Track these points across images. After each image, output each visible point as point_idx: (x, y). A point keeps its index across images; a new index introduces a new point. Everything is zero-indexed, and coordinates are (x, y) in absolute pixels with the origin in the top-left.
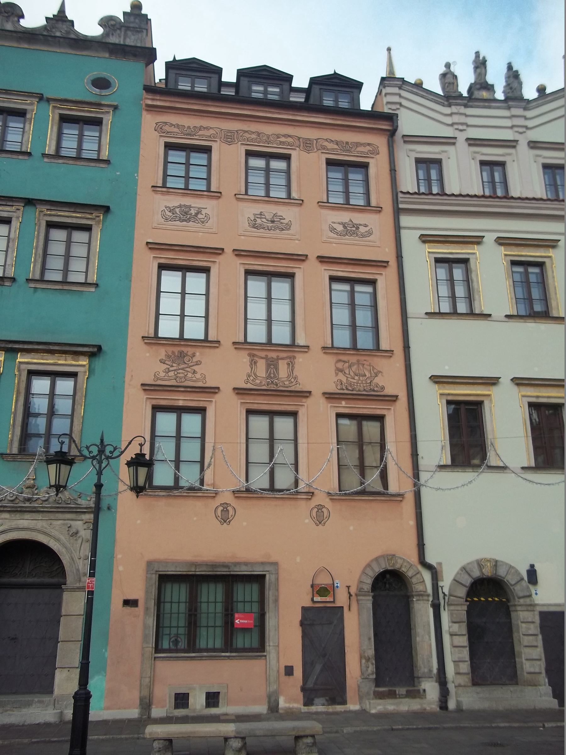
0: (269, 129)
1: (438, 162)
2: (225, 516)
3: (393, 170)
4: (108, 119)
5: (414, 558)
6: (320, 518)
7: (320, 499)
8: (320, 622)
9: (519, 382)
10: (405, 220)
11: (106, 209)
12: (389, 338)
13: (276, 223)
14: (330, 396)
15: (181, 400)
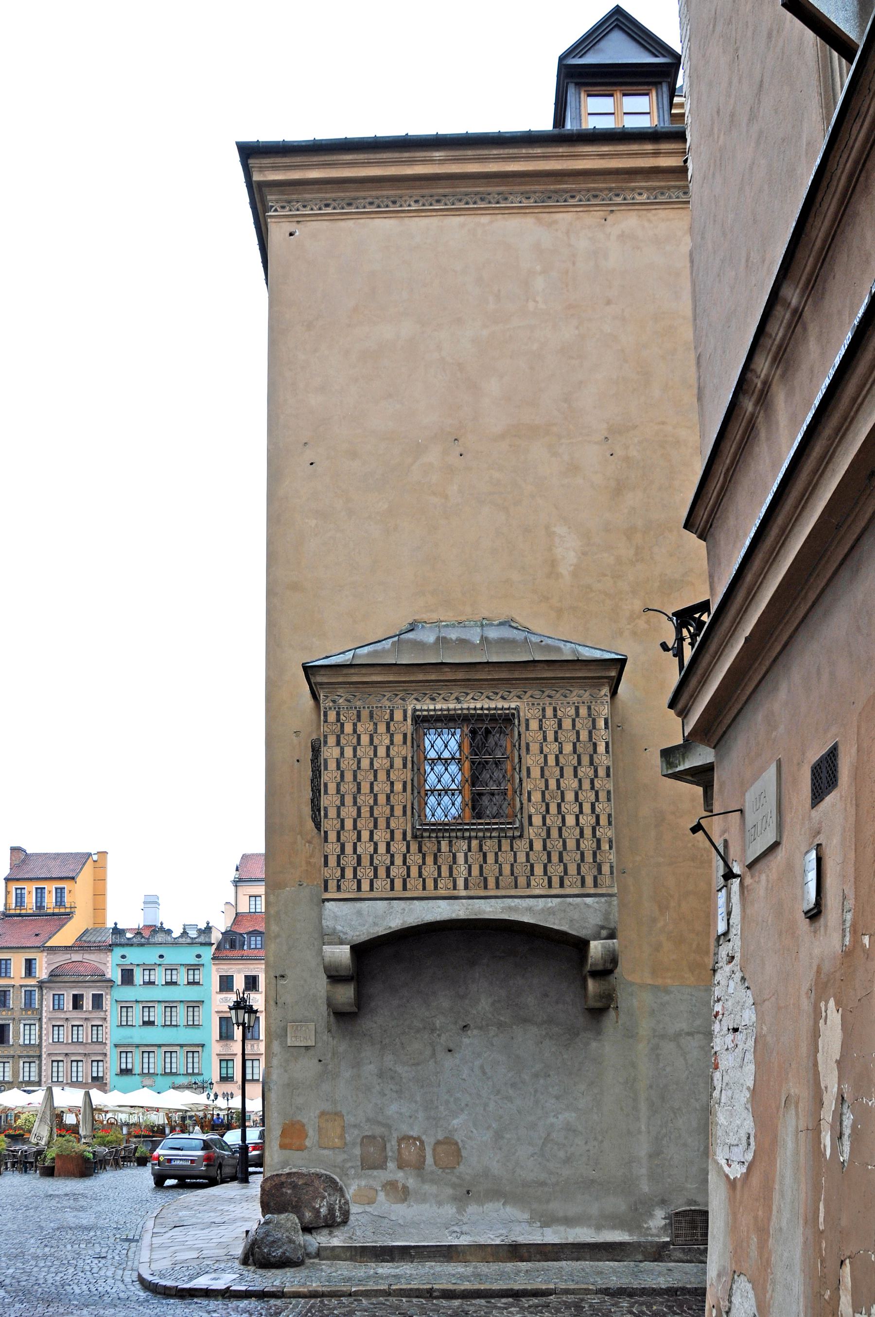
0: (252, 967)
4: (201, 969)
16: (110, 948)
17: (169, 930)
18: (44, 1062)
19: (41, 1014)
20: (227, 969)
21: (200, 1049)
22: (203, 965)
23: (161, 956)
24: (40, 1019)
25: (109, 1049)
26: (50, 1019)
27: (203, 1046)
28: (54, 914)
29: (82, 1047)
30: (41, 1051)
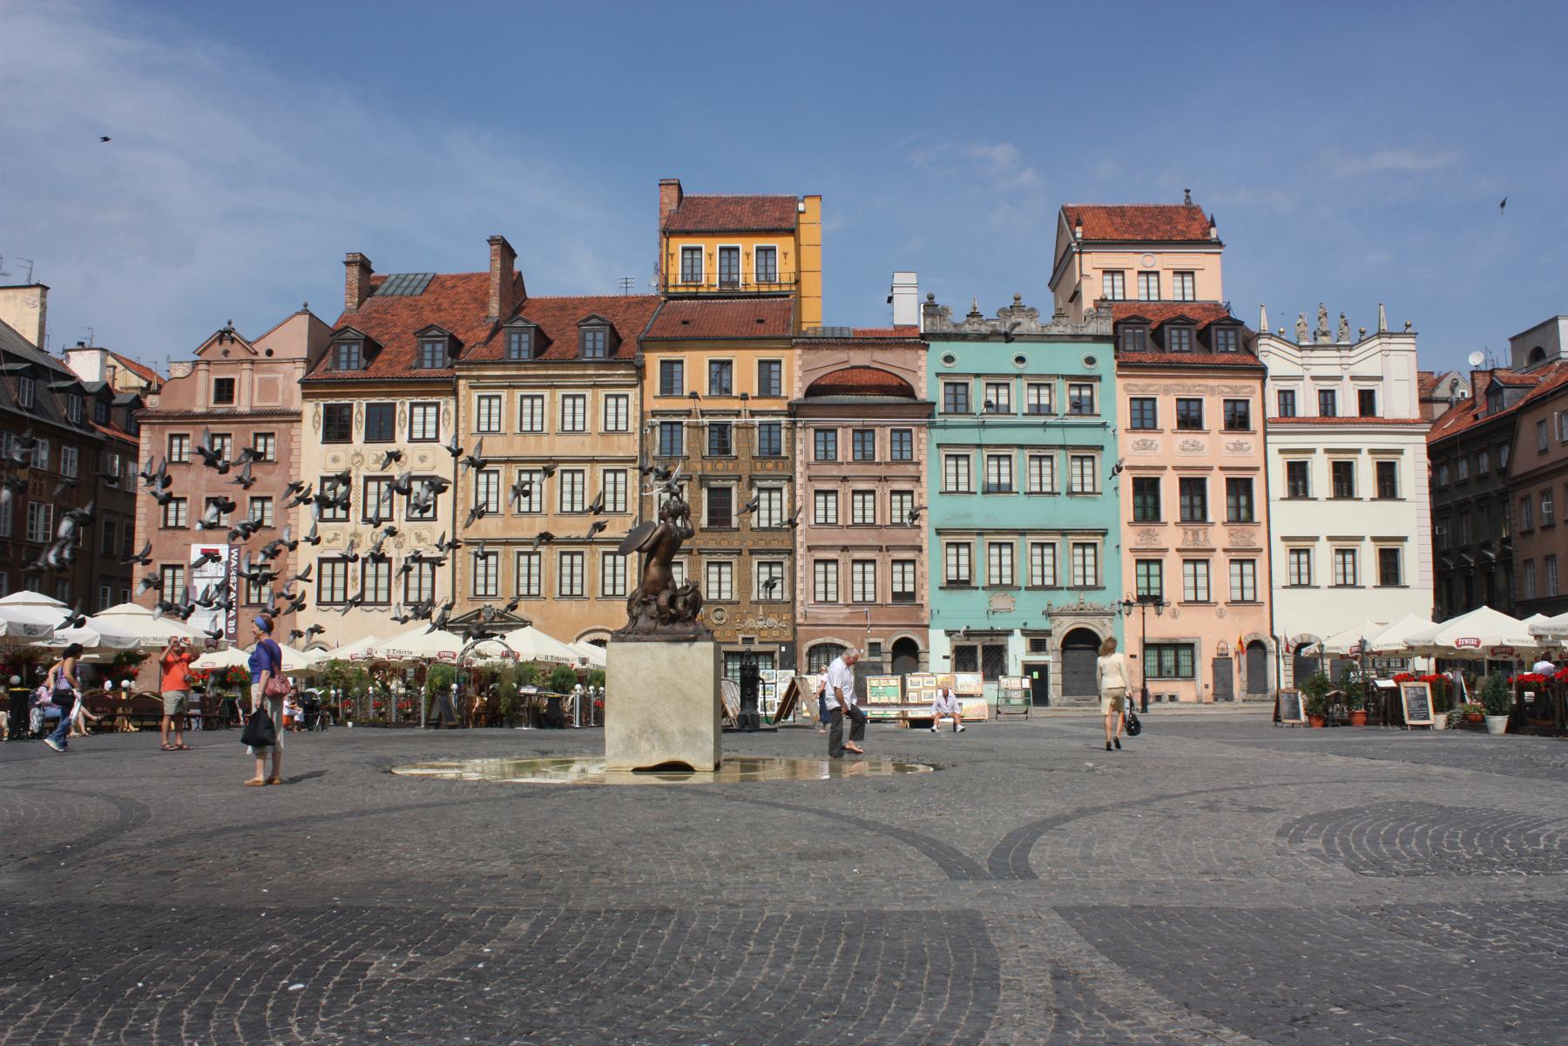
0: (1189, 382)
1: (1292, 392)
2: (1174, 616)
3: (1264, 406)
4: (1096, 385)
5: (1268, 634)
6: (1221, 616)
7: (1221, 605)
8: (1221, 665)
9: (1330, 538)
10: (1269, 438)
11: (1101, 448)
12: (1259, 514)
13: (1196, 447)
14: (1225, 550)
15: (1151, 556)
16: (921, 341)
17: (1032, 310)
18: (799, 563)
19: (793, 468)
20: (1145, 385)
21: (1098, 540)
22: (1099, 378)
23: (1020, 359)
24: (791, 480)
25: (927, 537)
26: (810, 479)
27: (1104, 533)
28: (759, 295)
29: (873, 532)
30: (794, 542)
